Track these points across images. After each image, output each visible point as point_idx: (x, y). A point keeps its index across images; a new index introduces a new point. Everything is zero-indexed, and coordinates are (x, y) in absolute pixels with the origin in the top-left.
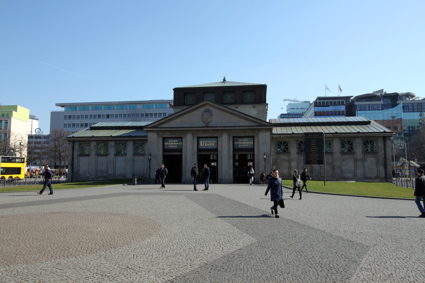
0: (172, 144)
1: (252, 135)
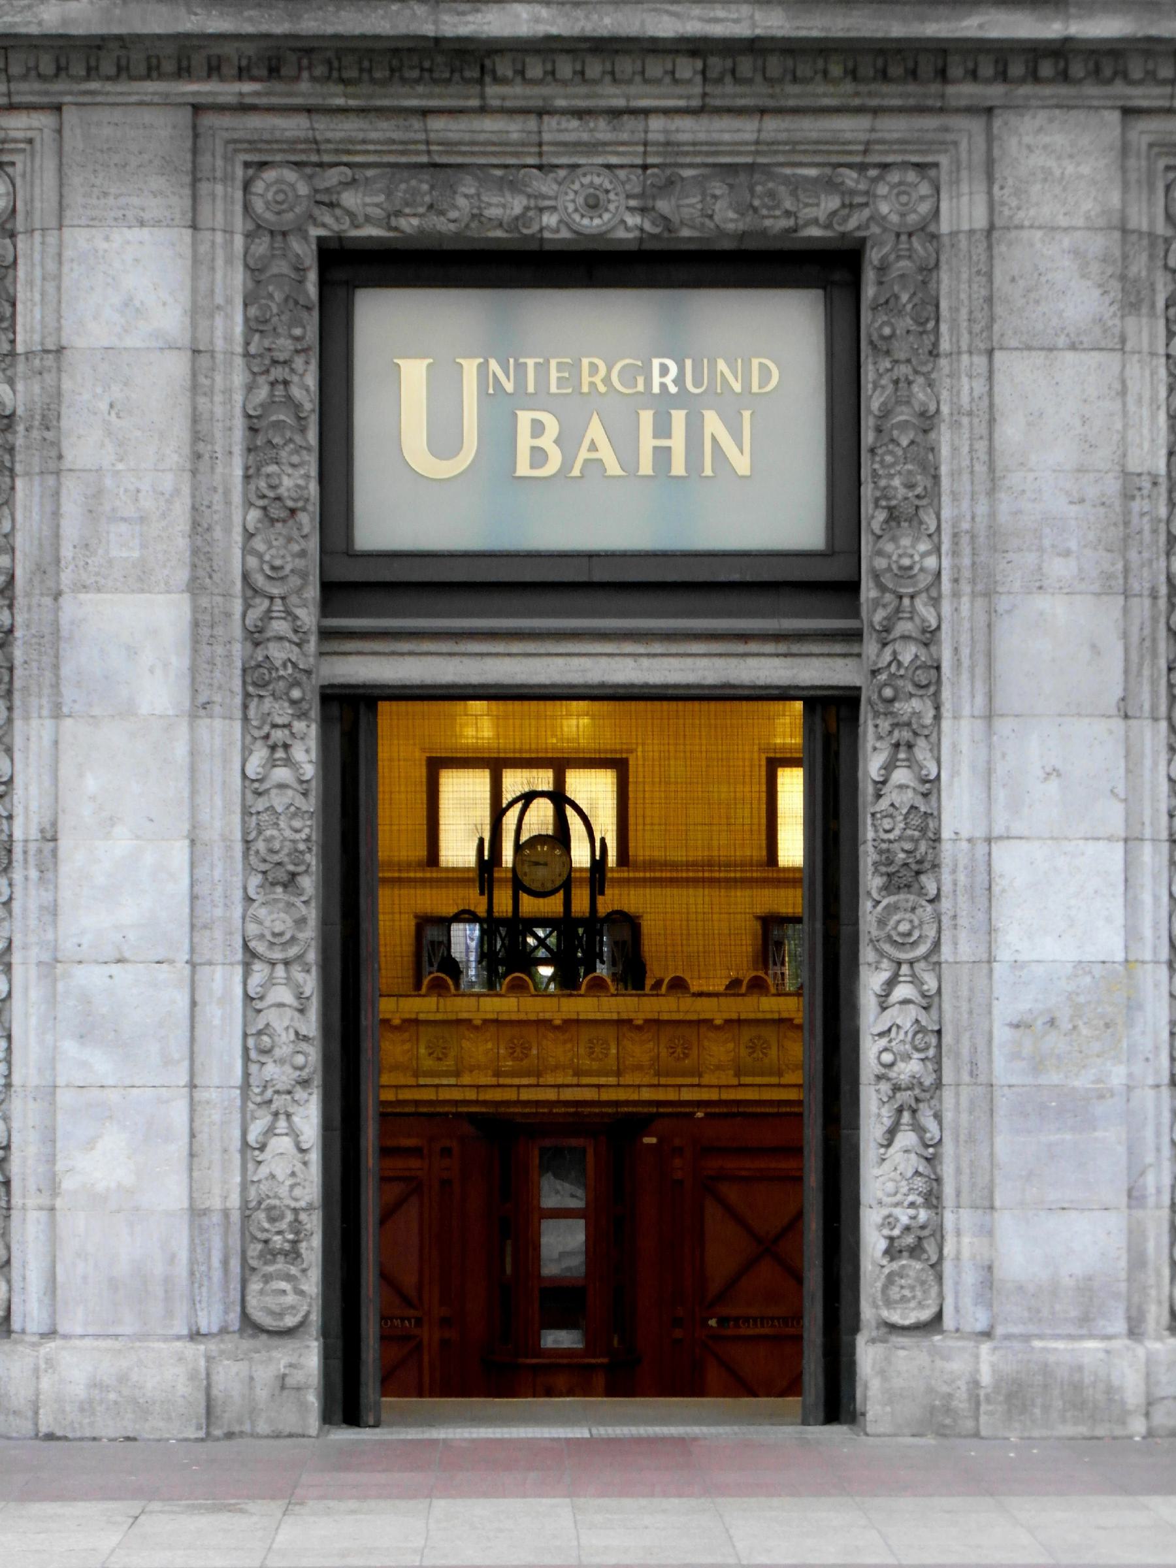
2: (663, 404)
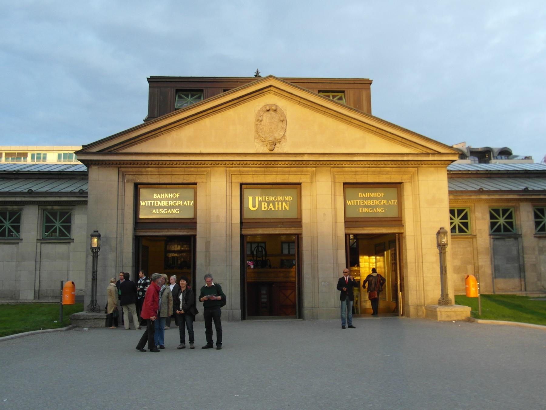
0: (164, 203)
1: (395, 179)
2: (278, 202)
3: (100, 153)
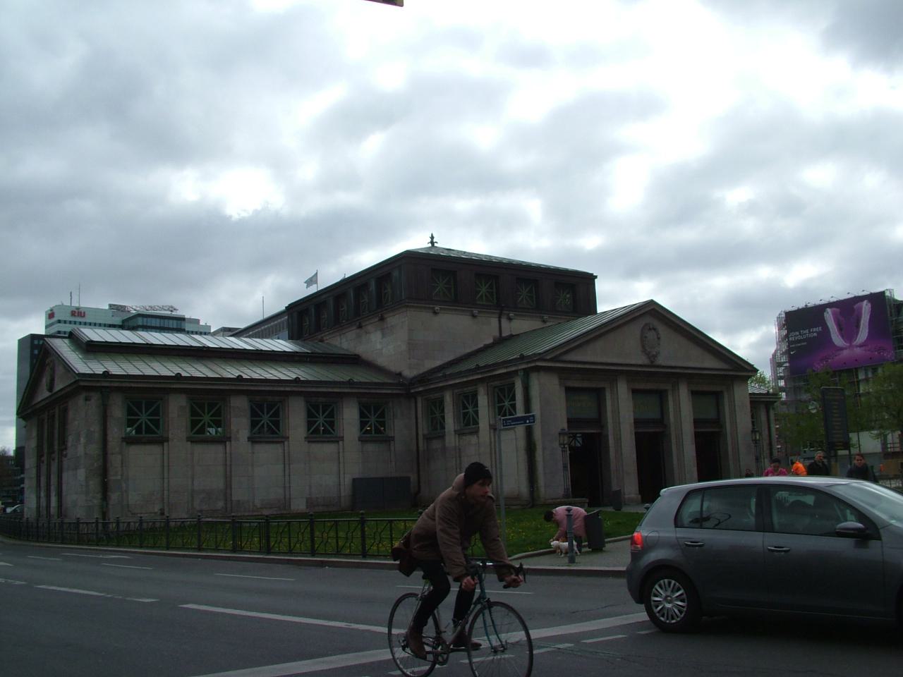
1: (718, 389)
3: (552, 360)
